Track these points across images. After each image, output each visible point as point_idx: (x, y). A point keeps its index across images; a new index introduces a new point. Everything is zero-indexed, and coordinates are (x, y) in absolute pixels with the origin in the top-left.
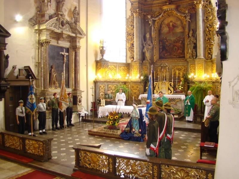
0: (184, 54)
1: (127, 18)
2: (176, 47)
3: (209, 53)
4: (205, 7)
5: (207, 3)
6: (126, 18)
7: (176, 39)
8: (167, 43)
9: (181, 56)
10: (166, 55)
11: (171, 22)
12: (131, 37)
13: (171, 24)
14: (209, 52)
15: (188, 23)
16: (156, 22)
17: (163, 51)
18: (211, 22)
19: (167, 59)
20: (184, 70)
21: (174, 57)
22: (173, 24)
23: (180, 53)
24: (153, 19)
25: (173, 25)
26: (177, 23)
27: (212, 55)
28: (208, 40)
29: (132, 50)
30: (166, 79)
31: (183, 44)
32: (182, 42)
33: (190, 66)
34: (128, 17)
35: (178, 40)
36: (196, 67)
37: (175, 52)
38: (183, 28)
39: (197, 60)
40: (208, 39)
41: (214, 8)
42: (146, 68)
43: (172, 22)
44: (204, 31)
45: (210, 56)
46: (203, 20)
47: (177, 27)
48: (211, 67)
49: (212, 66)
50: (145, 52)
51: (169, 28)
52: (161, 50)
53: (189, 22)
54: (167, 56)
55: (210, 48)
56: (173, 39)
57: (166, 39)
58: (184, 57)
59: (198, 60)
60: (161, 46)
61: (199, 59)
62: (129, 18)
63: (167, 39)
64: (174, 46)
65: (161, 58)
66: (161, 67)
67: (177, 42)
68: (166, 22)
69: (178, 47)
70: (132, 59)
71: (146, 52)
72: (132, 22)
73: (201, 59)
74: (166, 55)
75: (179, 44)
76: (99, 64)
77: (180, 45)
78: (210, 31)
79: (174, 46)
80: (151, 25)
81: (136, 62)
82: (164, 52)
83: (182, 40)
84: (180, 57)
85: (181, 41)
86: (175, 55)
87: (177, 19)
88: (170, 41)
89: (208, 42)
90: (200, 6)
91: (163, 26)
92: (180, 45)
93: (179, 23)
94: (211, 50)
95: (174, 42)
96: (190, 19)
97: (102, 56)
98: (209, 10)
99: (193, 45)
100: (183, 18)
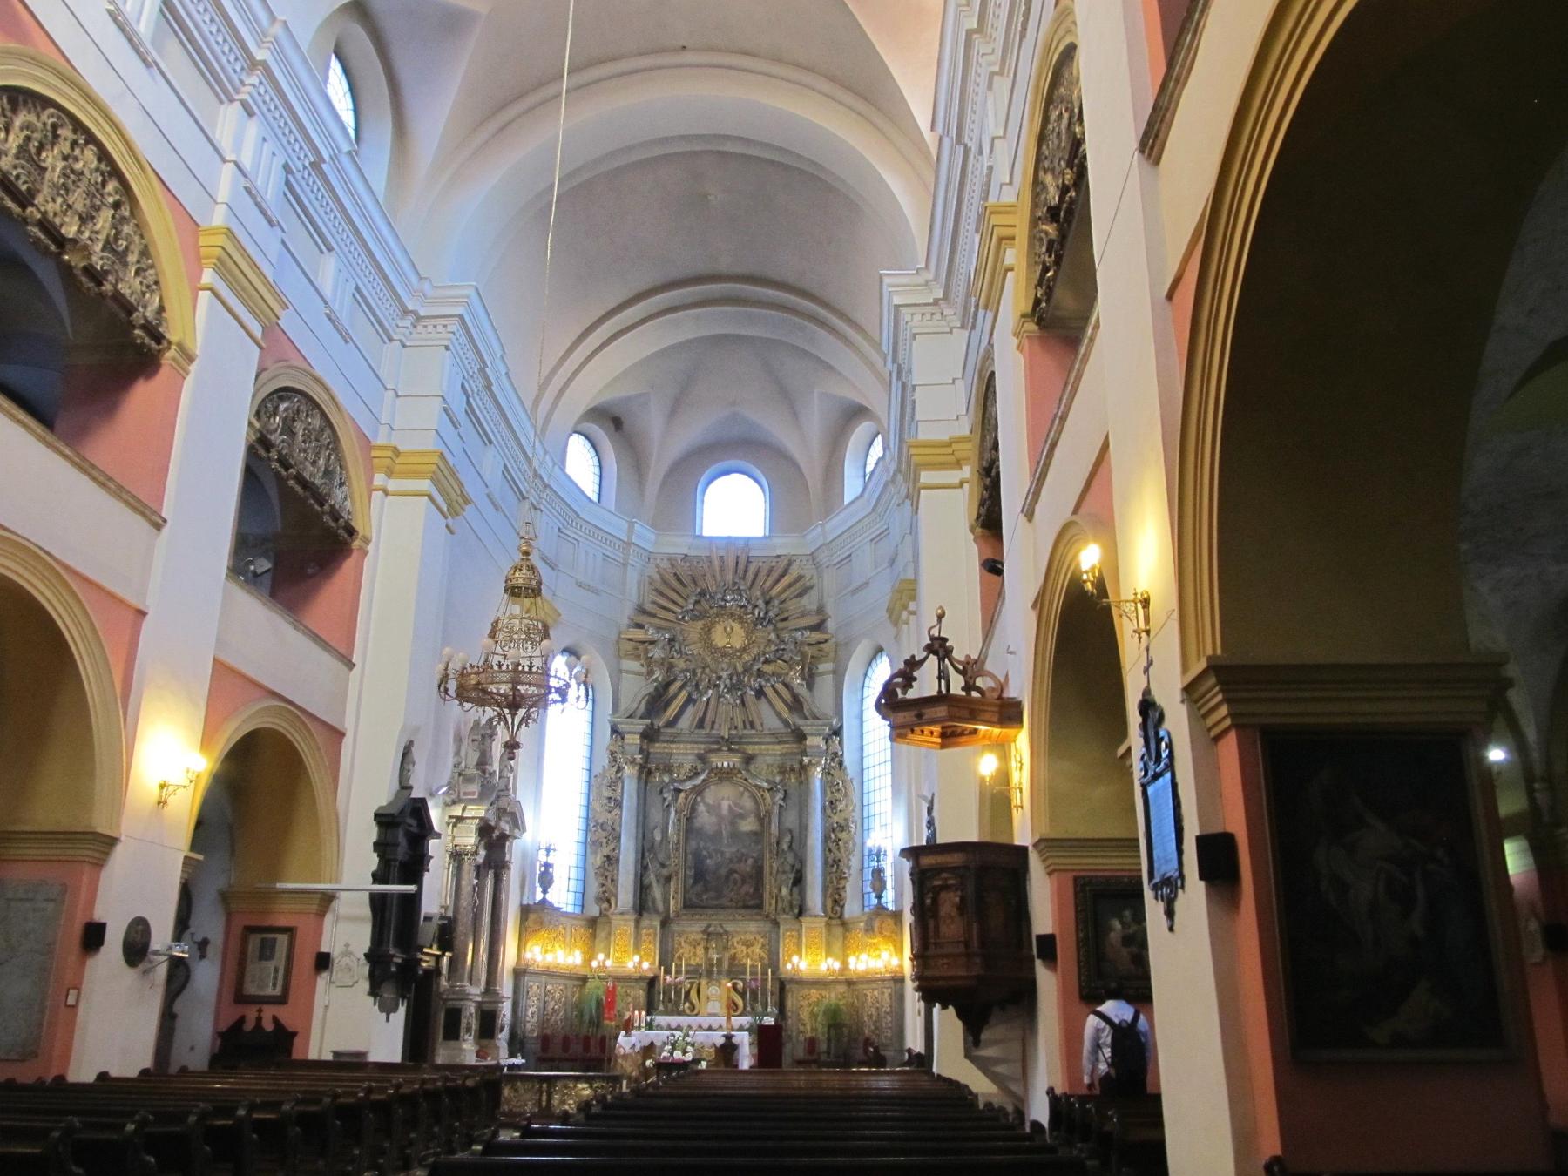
0: (761, 897)
1: (595, 772)
3: (836, 902)
4: (827, 772)
6: (590, 770)
9: (752, 903)
13: (725, 805)
16: (683, 795)
17: (695, 883)
18: (843, 815)
19: (710, 912)
30: (719, 973)
32: (756, 861)
34: (597, 770)
39: (805, 920)
44: (826, 839)
46: (824, 809)
47: (742, 817)
49: (845, 938)
58: (760, 906)
62: (603, 776)
64: (732, 872)
65: (688, 905)
67: (740, 861)
68: (710, 795)
70: (605, 905)
71: (654, 884)
76: (532, 916)
82: (699, 888)
84: (746, 907)
90: (817, 774)
91: (701, 808)
93: (748, 803)
97: (545, 891)
99: (792, 876)
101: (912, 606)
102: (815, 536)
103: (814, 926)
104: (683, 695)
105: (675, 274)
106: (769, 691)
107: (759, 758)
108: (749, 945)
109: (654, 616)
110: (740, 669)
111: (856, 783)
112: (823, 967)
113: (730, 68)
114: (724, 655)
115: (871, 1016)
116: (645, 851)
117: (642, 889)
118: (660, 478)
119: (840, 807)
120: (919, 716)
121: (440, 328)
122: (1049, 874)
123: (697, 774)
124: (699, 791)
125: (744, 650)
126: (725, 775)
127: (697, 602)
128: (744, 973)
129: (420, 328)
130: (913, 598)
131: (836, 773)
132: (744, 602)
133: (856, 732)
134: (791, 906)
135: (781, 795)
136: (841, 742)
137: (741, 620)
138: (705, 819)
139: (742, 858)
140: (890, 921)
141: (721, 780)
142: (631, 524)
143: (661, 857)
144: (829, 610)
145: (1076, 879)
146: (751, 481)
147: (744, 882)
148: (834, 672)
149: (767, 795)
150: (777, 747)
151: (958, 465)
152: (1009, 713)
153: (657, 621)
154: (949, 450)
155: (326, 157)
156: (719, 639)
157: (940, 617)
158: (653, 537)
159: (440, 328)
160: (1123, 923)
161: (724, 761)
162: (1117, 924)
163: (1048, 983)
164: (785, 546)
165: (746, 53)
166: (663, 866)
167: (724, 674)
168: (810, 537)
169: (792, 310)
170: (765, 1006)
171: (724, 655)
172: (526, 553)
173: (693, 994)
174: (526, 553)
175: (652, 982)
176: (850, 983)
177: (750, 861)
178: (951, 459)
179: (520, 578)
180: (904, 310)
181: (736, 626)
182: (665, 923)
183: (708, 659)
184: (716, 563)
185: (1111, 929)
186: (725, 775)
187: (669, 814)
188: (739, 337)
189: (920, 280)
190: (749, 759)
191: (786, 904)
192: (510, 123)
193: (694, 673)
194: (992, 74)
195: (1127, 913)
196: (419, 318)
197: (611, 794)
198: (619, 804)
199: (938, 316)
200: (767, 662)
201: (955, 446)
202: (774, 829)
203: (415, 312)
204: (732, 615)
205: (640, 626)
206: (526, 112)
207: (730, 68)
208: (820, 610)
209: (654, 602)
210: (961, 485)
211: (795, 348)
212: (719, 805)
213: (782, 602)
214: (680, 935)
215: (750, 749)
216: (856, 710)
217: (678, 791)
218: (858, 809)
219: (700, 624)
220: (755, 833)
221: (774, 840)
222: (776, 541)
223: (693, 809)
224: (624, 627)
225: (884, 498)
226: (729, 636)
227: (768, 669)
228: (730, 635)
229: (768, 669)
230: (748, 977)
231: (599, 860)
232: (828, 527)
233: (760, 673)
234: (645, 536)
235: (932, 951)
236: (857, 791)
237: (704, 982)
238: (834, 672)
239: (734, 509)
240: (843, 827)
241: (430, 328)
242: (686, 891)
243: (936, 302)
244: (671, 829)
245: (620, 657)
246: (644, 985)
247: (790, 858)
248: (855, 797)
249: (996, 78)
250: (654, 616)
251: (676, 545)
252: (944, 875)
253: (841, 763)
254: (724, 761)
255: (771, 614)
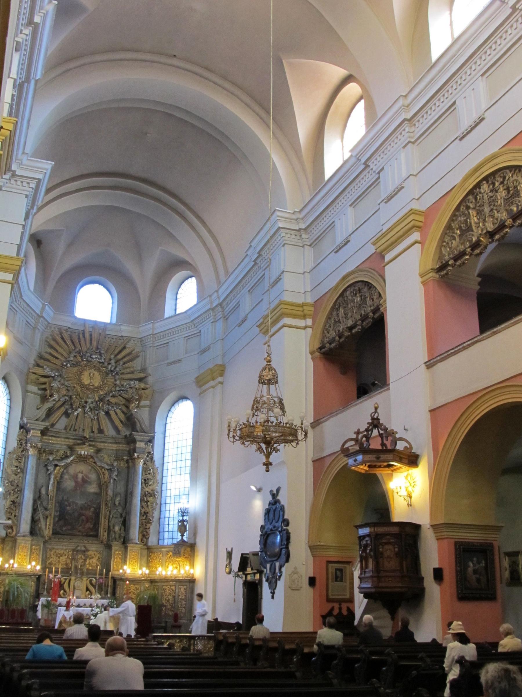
0: (97, 531)
2: (83, 517)
3: (144, 536)
5: (148, 459)
6: (5, 449)
7: (85, 503)
8: (68, 508)
9: (91, 533)
10: (64, 529)
11: (79, 472)
12: (12, 488)
13: (80, 476)
14: (145, 533)
15: (112, 481)
16: (58, 468)
17: (59, 520)
18: (151, 487)
19: (68, 537)
20: (97, 558)
21: (78, 533)
22: (83, 477)
23: (89, 528)
24: (56, 462)
25: (83, 480)
26: (90, 476)
27: (147, 539)
28: (144, 516)
29: (12, 514)
31: (97, 514)
32: (95, 510)
33: (114, 553)
34: (10, 449)
35: (88, 505)
36: (128, 557)
37: (81, 526)
38: (100, 486)
40: (144, 513)
41: (157, 468)
42: (37, 549)
43: (82, 473)
45: (145, 540)
47: (90, 483)
48: (146, 557)
50: (39, 519)
51: (76, 482)
52: (57, 519)
53: (114, 479)
54: (65, 530)
55: (147, 527)
56: (80, 502)
57: (67, 501)
58: (96, 536)
59: (132, 545)
60: (57, 511)
61: (133, 543)
63: (71, 500)
64: (81, 515)
65: (55, 533)
66: (77, 551)
68: (72, 470)
69: (87, 519)
70: (10, 530)
72: (17, 460)
73: (137, 544)
74: (64, 529)
75: (90, 513)
77: (91, 514)
78: (148, 501)
79: (81, 515)
80: (49, 472)
81: (26, 538)
82: (61, 523)
83: (95, 506)
84: (87, 536)
85: (94, 507)
86: (80, 531)
87: (91, 470)
88: (74, 506)
89: (144, 518)
91: (66, 476)
92: (91, 514)
93: (93, 477)
94: (147, 530)
95: (81, 509)
96: (117, 476)
98: (150, 470)
100: (103, 471)
101: (220, 379)
102: (145, 329)
103: (134, 549)
104: (63, 409)
105: (105, 169)
106: (112, 413)
107: (105, 451)
108: (59, 556)
109: (49, 361)
110: (97, 399)
111: (160, 470)
112: (140, 572)
113: (196, 74)
114: (88, 389)
115: (168, 601)
116: (37, 499)
117: (34, 521)
118: (56, 280)
119: (151, 483)
120: (378, 458)
121: (25, 184)
122: (437, 539)
123: (67, 457)
124: (66, 466)
125: (99, 388)
126: (82, 459)
127: (75, 356)
128: (96, 574)
129: (12, 181)
130: (222, 375)
131: (149, 464)
132: (103, 360)
133: (161, 443)
134: (119, 537)
135: (116, 473)
136: (153, 447)
137: (99, 370)
138: (69, 484)
139: (88, 508)
140: (189, 549)
141: (80, 461)
142: (44, 305)
143: (45, 504)
144: (150, 371)
145: (456, 543)
146: (105, 290)
147: (87, 521)
148: (150, 406)
149: (106, 472)
150: (114, 445)
151: (304, 317)
152: (412, 460)
153: (51, 364)
154: (301, 309)
155: (33, 83)
156: (86, 381)
157: (376, 409)
158: (52, 314)
159: (25, 184)
160: (473, 564)
161: (84, 451)
162: (471, 564)
163: (433, 591)
164: (126, 330)
165: (207, 69)
166: (46, 509)
167: (89, 401)
168: (141, 329)
169: (165, 204)
170: (107, 594)
171: (88, 389)
172: (270, 361)
173: (66, 586)
174: (269, 361)
175: (39, 578)
176: (152, 582)
177: (92, 509)
178: (302, 313)
179: (268, 374)
180: (282, 230)
181: (97, 373)
182: (45, 542)
183: (79, 390)
184: (87, 336)
185: (469, 567)
186: (82, 459)
187: (49, 479)
188: (124, 210)
189: (294, 217)
190: (98, 451)
191: (117, 536)
192: (71, 69)
193: (71, 397)
194: (409, 142)
195: (475, 559)
196: (14, 175)
197: (17, 464)
198: (23, 471)
199: (298, 237)
200: (113, 396)
201: (305, 308)
202: (110, 492)
203: (14, 172)
204: (94, 366)
205: (38, 365)
206: (79, 66)
207: (196, 74)
208: (143, 370)
209: (46, 352)
210: (305, 328)
211: (155, 222)
212: (77, 475)
213: (124, 364)
214: (51, 550)
215: (100, 445)
216: (162, 429)
217: (56, 466)
218: (159, 485)
219: (76, 369)
220: (95, 494)
221: (109, 499)
222: (123, 328)
223: (61, 477)
224: (31, 366)
225: (204, 315)
226: (91, 378)
227: (113, 400)
228: (91, 378)
229: (113, 400)
230: (98, 577)
231: (8, 503)
232: (157, 325)
233: (109, 403)
234: (49, 313)
235: (382, 574)
236: (160, 475)
237: (73, 578)
238: (150, 406)
239: (95, 304)
240: (152, 494)
241: (19, 183)
242: (54, 525)
243: (299, 230)
244: (50, 488)
245: (27, 383)
246: (35, 580)
247: (120, 510)
248: (159, 478)
249: (410, 144)
250: (49, 361)
251: (64, 322)
252: (388, 537)
253: (152, 458)
254: (84, 451)
255: (118, 369)
